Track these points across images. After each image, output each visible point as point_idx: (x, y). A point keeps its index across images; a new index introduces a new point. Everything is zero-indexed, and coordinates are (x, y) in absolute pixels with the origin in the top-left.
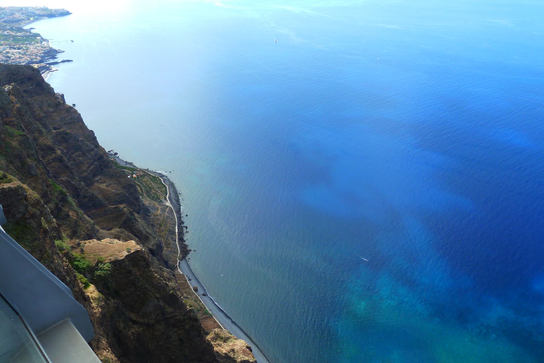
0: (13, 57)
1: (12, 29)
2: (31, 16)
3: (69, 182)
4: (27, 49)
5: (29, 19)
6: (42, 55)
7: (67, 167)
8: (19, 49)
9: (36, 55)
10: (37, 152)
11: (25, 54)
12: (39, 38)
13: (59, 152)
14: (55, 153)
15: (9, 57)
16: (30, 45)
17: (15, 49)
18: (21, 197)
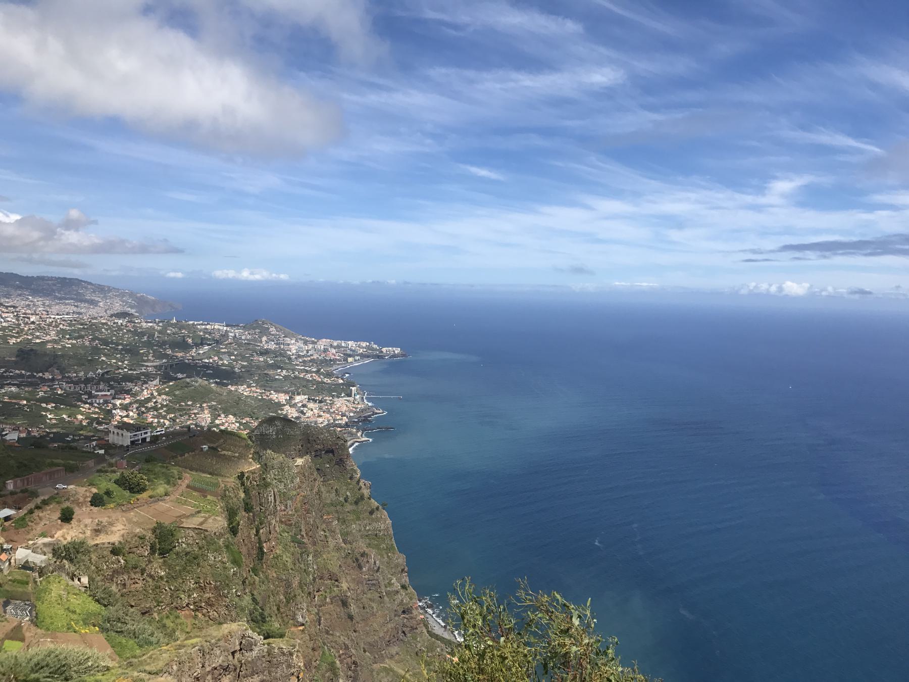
0: (309, 414)
1: (318, 372)
2: (350, 356)
3: (347, 648)
4: (332, 404)
5: (346, 360)
6: (352, 414)
7: (351, 617)
8: (321, 402)
9: (343, 415)
10: (314, 579)
11: (328, 412)
12: (353, 388)
13: (345, 586)
14: (338, 586)
15: (304, 414)
16: (338, 397)
17: (315, 401)
18: (292, 670)
